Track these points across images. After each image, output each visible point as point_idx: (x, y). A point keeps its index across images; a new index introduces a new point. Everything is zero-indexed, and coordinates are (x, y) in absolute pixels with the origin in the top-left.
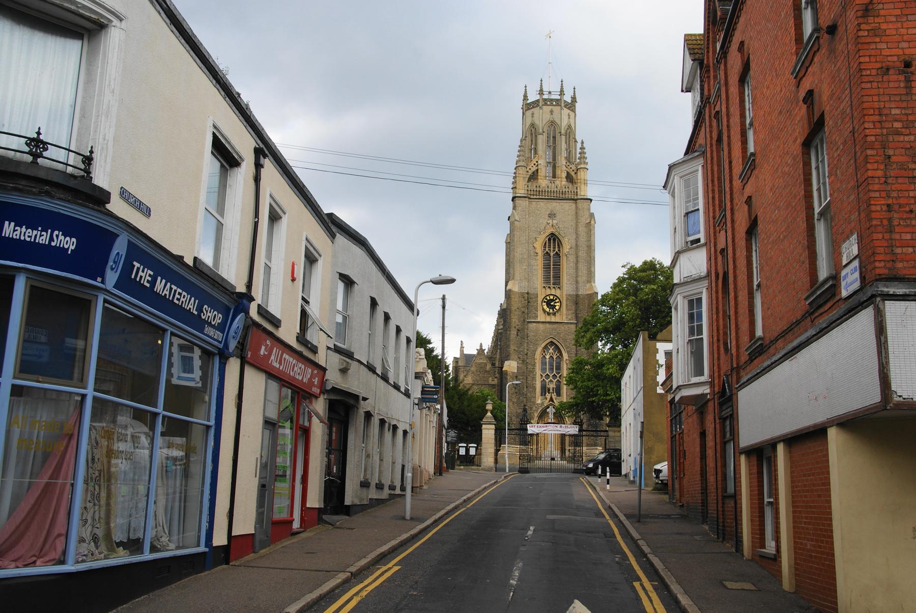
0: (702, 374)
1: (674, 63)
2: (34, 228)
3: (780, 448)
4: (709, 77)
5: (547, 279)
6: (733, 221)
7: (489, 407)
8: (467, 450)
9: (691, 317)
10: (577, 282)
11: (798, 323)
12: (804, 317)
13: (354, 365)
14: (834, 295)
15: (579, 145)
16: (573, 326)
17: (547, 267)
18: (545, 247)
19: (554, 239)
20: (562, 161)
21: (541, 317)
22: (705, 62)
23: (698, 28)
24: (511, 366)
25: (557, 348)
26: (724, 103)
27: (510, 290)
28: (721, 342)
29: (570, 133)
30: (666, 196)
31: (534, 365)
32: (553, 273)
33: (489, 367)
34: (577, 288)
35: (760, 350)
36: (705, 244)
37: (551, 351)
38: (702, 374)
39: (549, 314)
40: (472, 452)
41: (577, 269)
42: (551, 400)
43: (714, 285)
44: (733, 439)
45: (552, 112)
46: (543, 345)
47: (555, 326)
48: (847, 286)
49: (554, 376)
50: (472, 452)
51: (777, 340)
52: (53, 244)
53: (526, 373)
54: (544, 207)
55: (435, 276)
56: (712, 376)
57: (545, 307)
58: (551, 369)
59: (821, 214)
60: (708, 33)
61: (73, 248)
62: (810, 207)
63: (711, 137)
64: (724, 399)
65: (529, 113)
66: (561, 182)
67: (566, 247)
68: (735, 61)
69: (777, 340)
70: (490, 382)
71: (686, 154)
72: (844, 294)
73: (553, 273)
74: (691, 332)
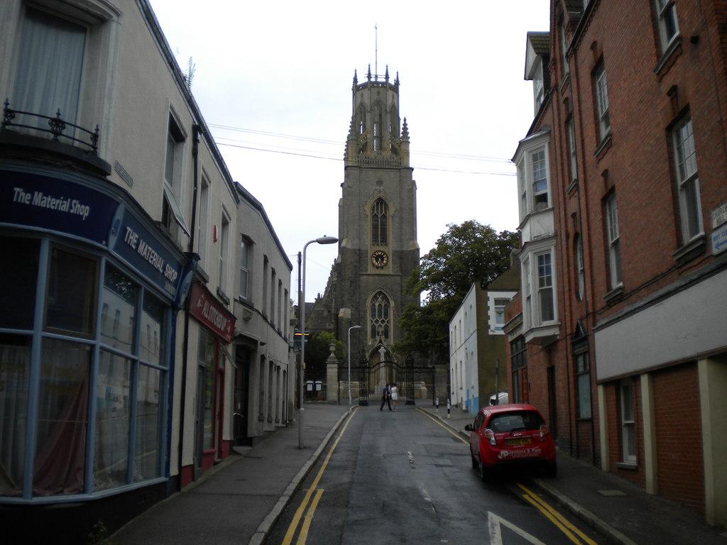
0: (551, 318)
1: (517, 55)
2: (57, 198)
3: (644, 380)
4: (555, 68)
6: (586, 190)
7: (332, 349)
8: (314, 387)
9: (541, 270)
11: (664, 275)
12: (670, 271)
13: (255, 313)
14: (704, 253)
15: (402, 122)
16: (398, 278)
17: (375, 227)
18: (373, 210)
19: (381, 202)
20: (387, 136)
21: (371, 270)
22: (552, 56)
23: (544, 25)
24: (345, 313)
25: (385, 298)
26: (575, 91)
27: (344, 247)
28: (573, 292)
29: (395, 110)
30: (513, 168)
31: (365, 312)
32: (380, 234)
33: (326, 313)
35: (617, 299)
36: (553, 209)
37: (380, 299)
38: (551, 318)
39: (377, 267)
40: (319, 388)
42: (381, 342)
43: (564, 243)
44: (589, 372)
45: (378, 93)
46: (373, 295)
47: (383, 278)
48: (717, 246)
49: (383, 321)
50: (319, 388)
51: (639, 289)
52: (72, 211)
53: (358, 318)
54: (372, 176)
55: (321, 236)
56: (560, 320)
57: (374, 261)
58: (380, 316)
59: (684, 186)
60: (555, 32)
61: (86, 214)
62: (674, 181)
63: (559, 119)
64: (580, 341)
65: (359, 94)
66: (388, 154)
67: (391, 211)
68: (586, 57)
69: (639, 289)
70: (327, 327)
71: (529, 134)
72: (715, 251)
73: (380, 234)
74: (541, 284)
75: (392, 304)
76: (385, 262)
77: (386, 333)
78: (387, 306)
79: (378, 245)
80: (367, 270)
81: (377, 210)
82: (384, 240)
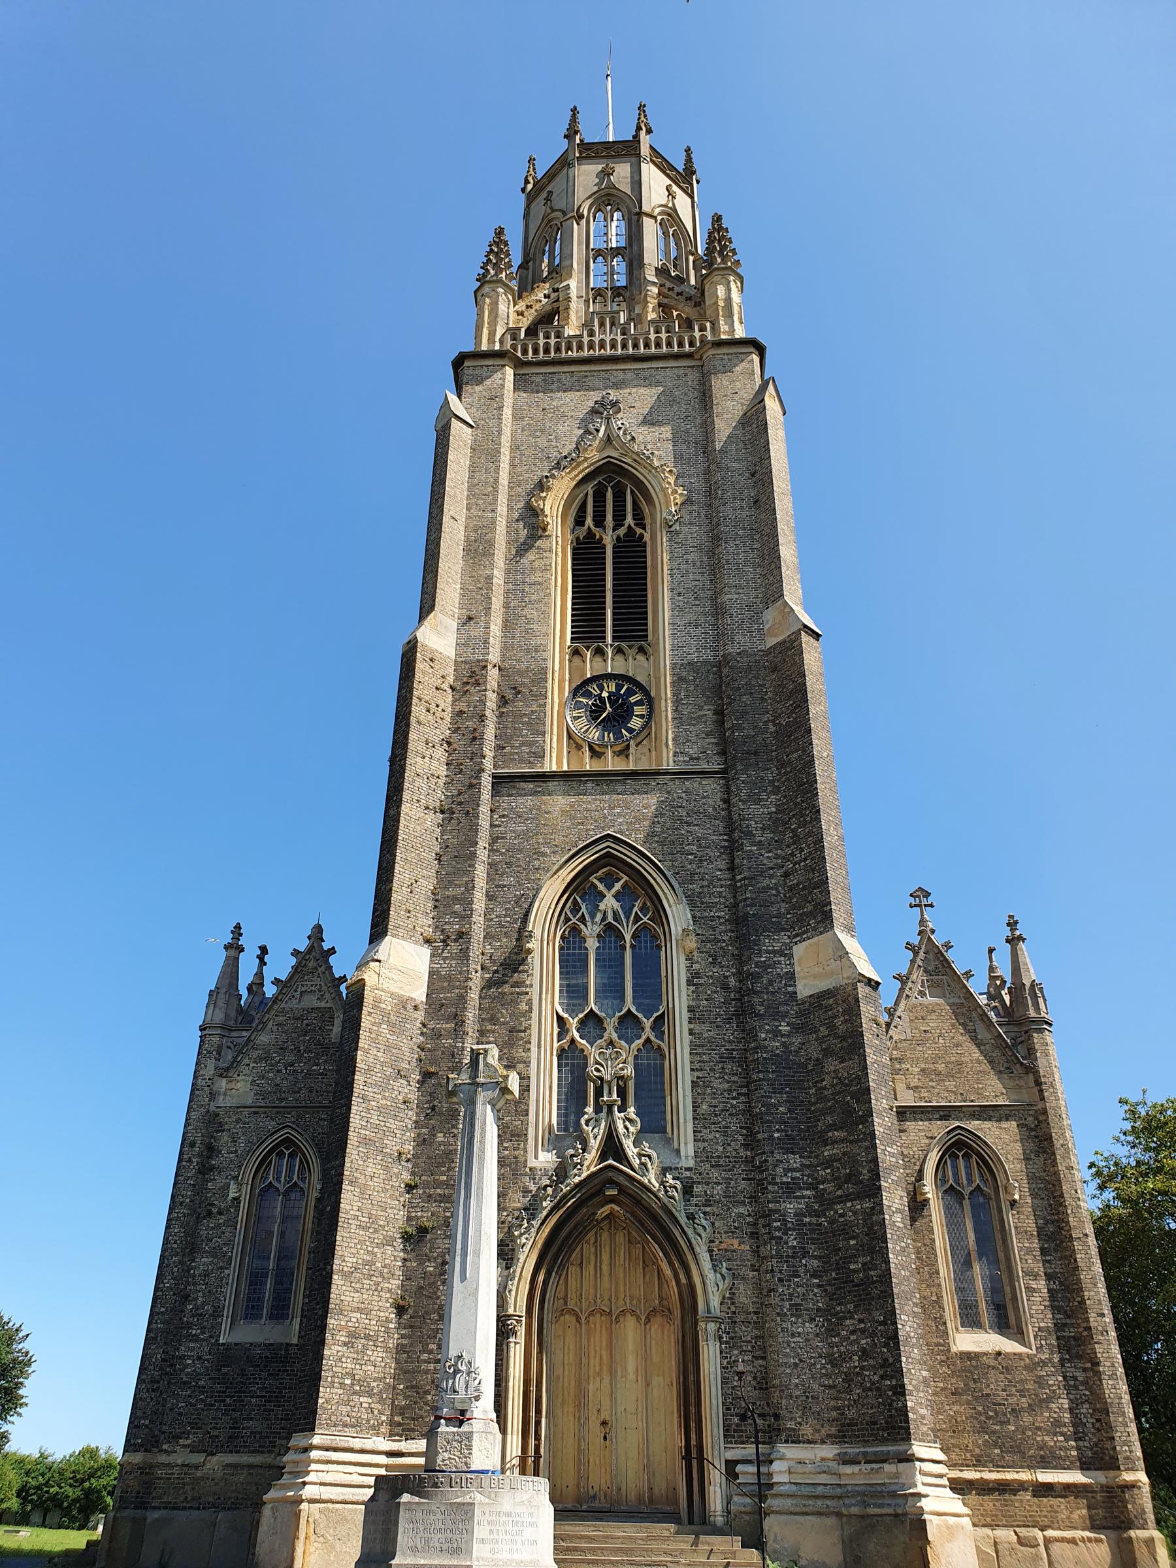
5: (586, 627)
10: (718, 611)
16: (711, 789)
18: (579, 521)
34: (720, 636)
37: (609, 903)
41: (714, 565)
46: (567, 874)
58: (612, 989)
75: (679, 916)
76: (636, 723)
77: (649, 1091)
78: (651, 941)
79: (599, 652)
80: (541, 756)
81: (599, 521)
82: (634, 628)
